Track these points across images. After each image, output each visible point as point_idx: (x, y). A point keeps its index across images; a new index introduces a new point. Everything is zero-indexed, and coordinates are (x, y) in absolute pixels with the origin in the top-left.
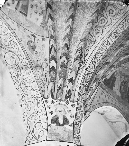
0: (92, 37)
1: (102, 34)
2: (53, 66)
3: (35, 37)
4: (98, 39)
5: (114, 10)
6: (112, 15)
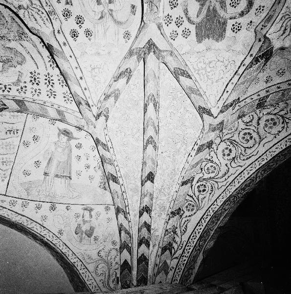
0: (193, 199)
1: (210, 194)
2: (126, 260)
3: (91, 210)
4: (204, 202)
5: (233, 149)
6: (229, 158)
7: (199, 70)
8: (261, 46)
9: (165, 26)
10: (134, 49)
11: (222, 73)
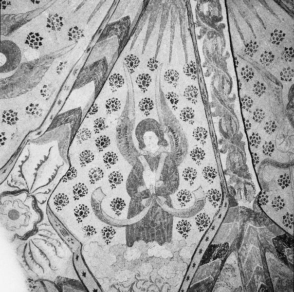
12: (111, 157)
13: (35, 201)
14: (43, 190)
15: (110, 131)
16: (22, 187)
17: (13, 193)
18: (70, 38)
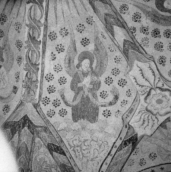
7: (74, 147)
8: (127, 132)
9: (42, 106)
10: (9, 122)
11: (97, 152)
12: (167, 33)
13: (160, 88)
14: (157, 81)
15: (151, 26)
16: (148, 90)
17: (148, 95)
18: (91, 24)
